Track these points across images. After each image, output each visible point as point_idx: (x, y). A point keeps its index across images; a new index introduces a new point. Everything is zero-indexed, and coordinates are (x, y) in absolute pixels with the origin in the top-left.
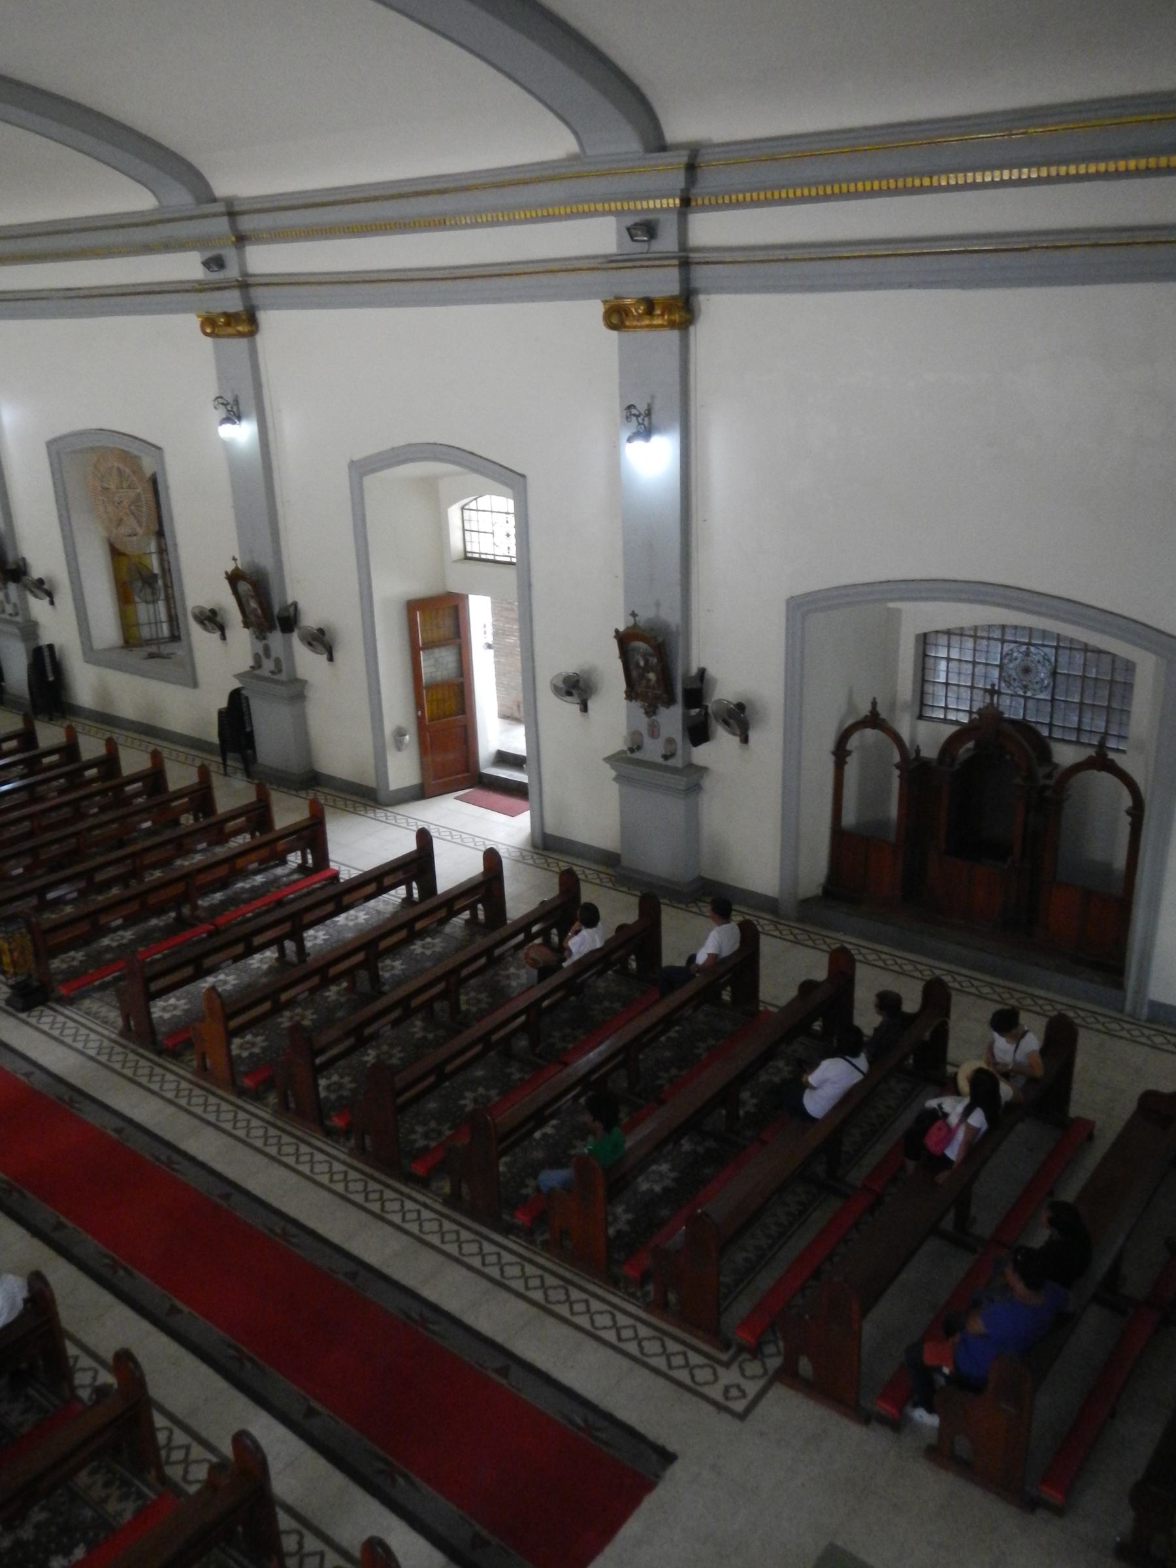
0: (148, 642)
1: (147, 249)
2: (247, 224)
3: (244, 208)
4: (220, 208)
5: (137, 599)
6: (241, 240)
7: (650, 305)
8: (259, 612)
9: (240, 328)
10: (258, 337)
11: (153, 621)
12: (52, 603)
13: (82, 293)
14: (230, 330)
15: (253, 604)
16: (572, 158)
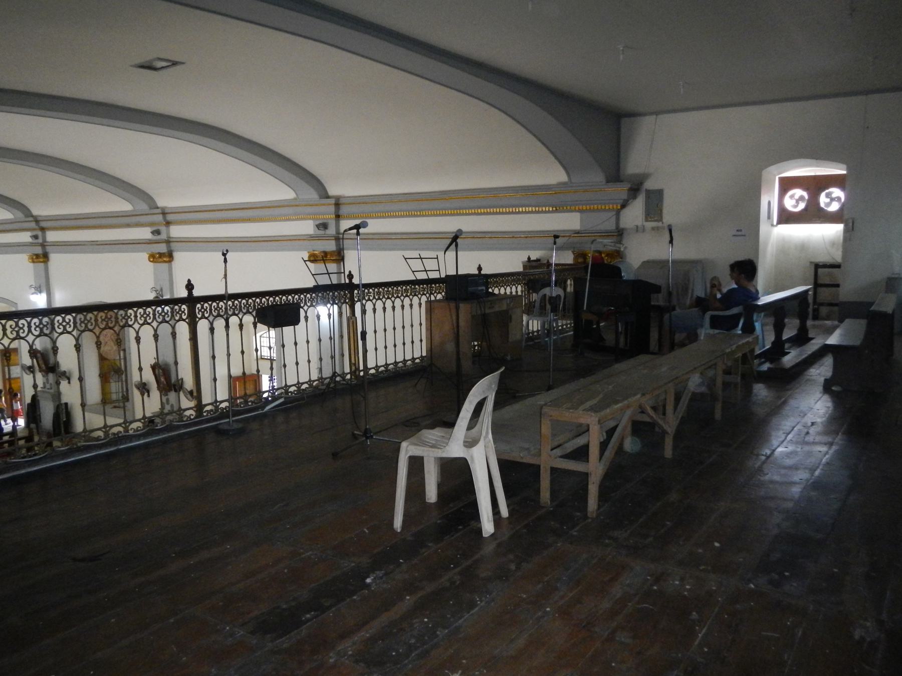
0: (114, 401)
1: (128, 226)
2: (170, 217)
3: (169, 211)
4: (159, 211)
5: (111, 381)
6: (168, 224)
7: (325, 254)
8: (165, 383)
9: (165, 259)
10: (173, 263)
11: (117, 391)
12: (69, 383)
13: (98, 243)
14: (160, 260)
15: (162, 379)
16: (295, 199)
